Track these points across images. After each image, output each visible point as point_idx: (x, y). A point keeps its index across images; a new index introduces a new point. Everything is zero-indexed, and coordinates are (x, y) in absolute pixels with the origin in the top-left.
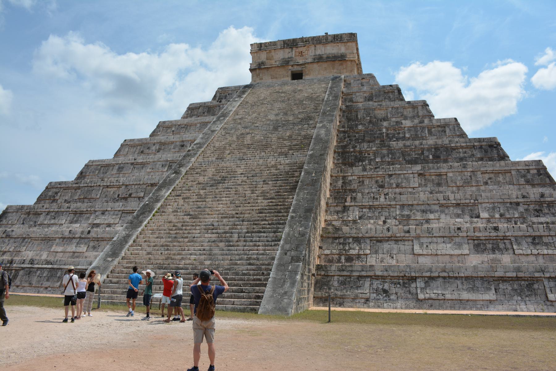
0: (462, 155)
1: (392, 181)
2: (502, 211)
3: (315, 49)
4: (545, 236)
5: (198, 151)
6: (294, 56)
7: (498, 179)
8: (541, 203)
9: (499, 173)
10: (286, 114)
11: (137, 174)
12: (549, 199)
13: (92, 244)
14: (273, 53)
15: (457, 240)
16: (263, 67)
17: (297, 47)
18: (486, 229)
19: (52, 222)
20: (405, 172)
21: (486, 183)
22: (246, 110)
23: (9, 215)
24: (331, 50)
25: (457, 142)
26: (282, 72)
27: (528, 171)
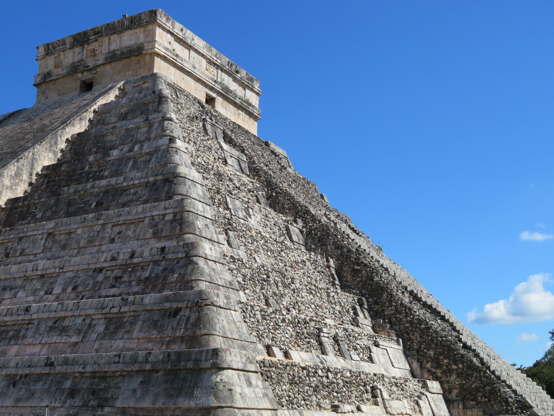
1: (19, 247)
2: (78, 283)
3: (109, 43)
4: (69, 317)
7: (129, 232)
8: (124, 267)
9: (132, 223)
12: (135, 260)
14: (62, 57)
16: (48, 80)
17: (89, 44)
18: (18, 311)
20: (35, 233)
21: (112, 241)
24: (128, 39)
25: (132, 179)
27: (164, 215)
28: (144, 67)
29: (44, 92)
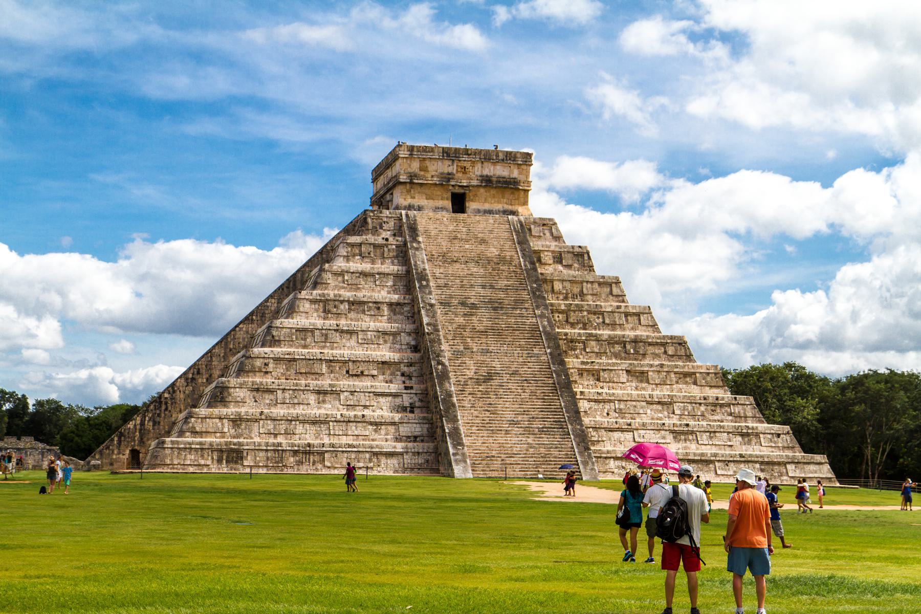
0: (657, 351)
5: (439, 335)
6: (455, 172)
8: (715, 405)
10: (492, 287)
11: (348, 345)
13: (370, 427)
14: (428, 163)
15: (663, 432)
16: (416, 181)
19: (296, 401)
21: (677, 382)
22: (441, 271)
23: (232, 390)
24: (500, 171)
26: (438, 192)
28: (518, 199)
29: (409, 191)
